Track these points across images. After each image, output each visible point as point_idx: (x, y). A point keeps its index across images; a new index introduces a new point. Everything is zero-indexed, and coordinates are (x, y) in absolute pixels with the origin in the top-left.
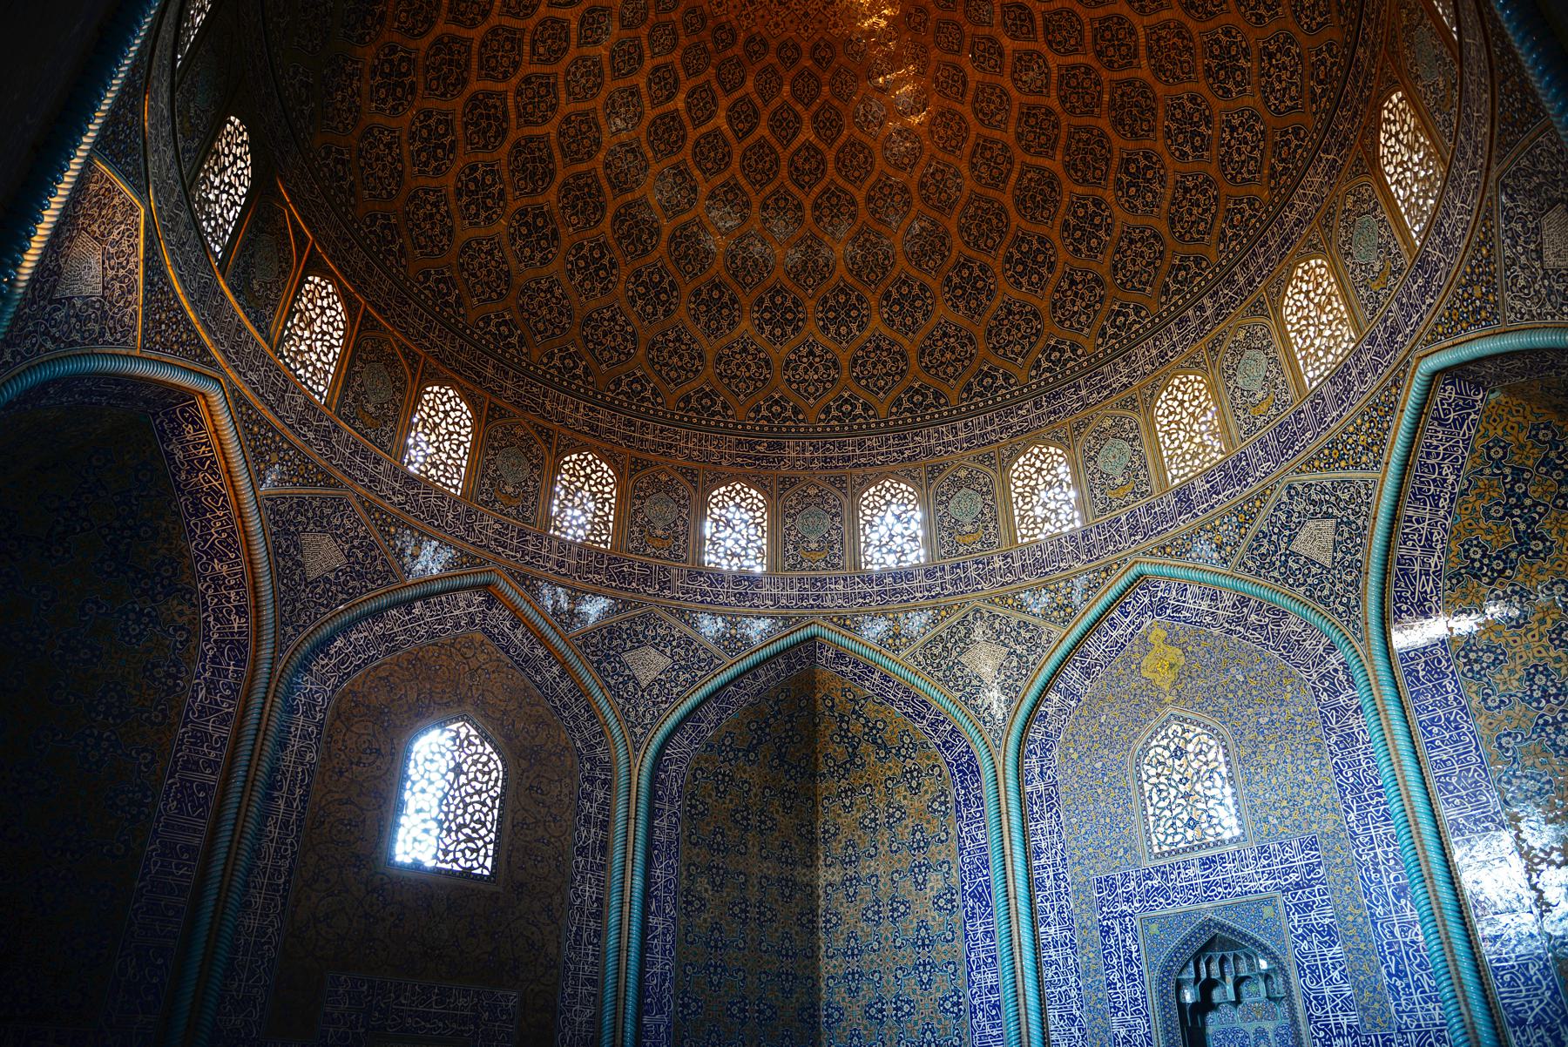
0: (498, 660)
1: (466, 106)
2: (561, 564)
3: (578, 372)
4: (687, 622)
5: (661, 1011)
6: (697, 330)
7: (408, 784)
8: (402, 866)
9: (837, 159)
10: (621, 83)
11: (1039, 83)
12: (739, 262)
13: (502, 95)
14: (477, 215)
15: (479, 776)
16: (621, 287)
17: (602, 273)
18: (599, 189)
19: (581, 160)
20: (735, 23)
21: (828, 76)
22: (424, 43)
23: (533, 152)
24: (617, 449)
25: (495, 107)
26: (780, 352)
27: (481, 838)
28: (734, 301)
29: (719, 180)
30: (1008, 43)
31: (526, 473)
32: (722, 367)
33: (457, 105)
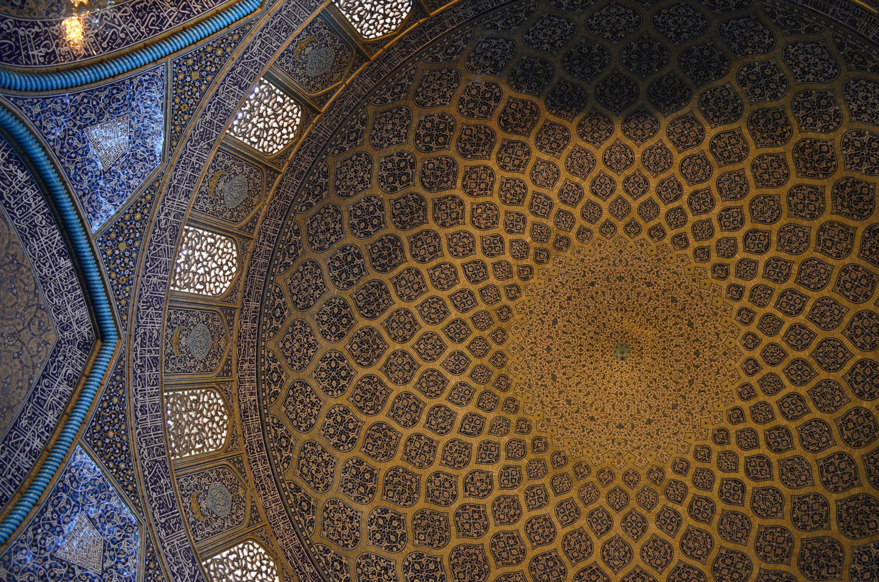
0: (34, 366)
1: (391, 235)
3: (273, 387)
4: (148, 568)
6: (339, 476)
9: (498, 499)
10: (443, 336)
11: (659, 562)
12: (396, 480)
13: (404, 260)
14: (335, 268)
16: (332, 402)
17: (334, 383)
18: (379, 356)
19: (390, 335)
20: (513, 385)
21: (533, 456)
22: (418, 189)
23: (381, 296)
24: (240, 440)
25: (396, 258)
26: (367, 546)
28: (372, 492)
29: (430, 434)
30: (653, 528)
31: (198, 357)
32: (331, 507)
33: (391, 229)
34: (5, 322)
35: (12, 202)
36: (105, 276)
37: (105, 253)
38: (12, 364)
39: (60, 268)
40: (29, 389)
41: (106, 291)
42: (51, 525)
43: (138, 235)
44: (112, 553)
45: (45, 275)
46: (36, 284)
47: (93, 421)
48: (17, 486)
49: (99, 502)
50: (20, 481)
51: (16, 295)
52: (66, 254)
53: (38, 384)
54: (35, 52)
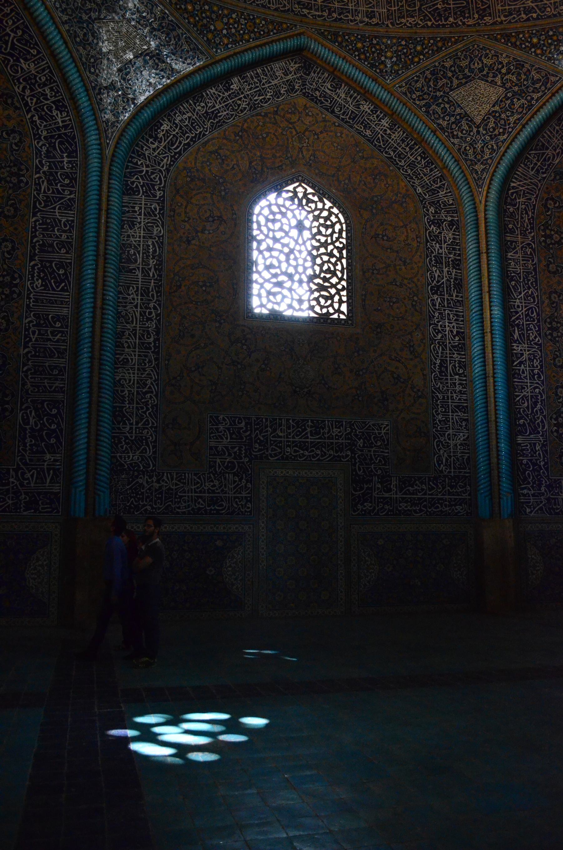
0: (324, 120)
2: (371, 15)
4: (514, 45)
5: (535, 431)
7: (255, 244)
8: (261, 317)
15: (323, 230)
27: (333, 286)
34: (291, 146)
35: (191, 135)
36: (247, 47)
37: (227, 45)
38: (323, 141)
39: (240, 89)
40: (342, 126)
41: (261, 46)
42: (453, 123)
43: (207, 7)
44: (491, 75)
45: (248, 105)
46: (257, 115)
47: (375, 71)
48: (415, 143)
49: (445, 78)
50: (412, 140)
51: (268, 134)
52: (227, 83)
53: (338, 117)
54: (59, 120)
